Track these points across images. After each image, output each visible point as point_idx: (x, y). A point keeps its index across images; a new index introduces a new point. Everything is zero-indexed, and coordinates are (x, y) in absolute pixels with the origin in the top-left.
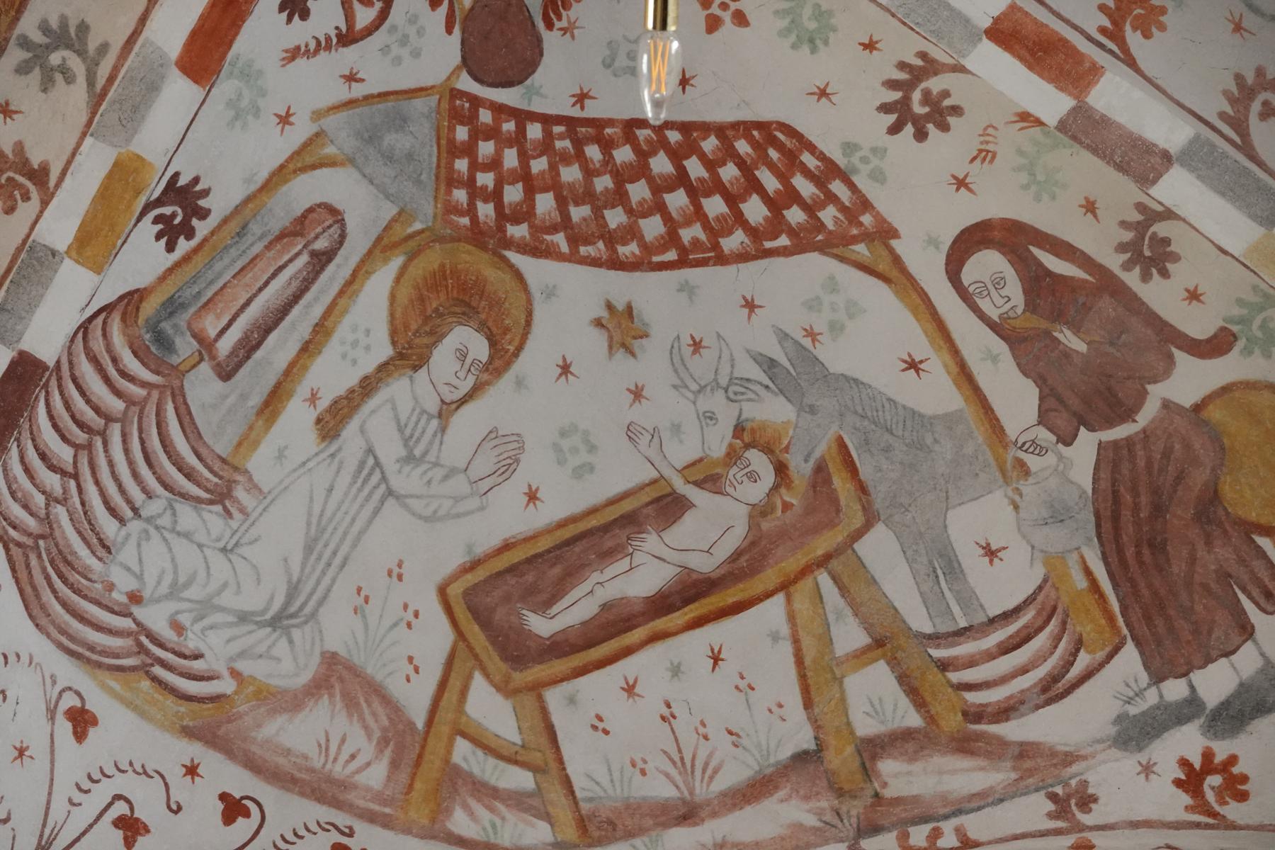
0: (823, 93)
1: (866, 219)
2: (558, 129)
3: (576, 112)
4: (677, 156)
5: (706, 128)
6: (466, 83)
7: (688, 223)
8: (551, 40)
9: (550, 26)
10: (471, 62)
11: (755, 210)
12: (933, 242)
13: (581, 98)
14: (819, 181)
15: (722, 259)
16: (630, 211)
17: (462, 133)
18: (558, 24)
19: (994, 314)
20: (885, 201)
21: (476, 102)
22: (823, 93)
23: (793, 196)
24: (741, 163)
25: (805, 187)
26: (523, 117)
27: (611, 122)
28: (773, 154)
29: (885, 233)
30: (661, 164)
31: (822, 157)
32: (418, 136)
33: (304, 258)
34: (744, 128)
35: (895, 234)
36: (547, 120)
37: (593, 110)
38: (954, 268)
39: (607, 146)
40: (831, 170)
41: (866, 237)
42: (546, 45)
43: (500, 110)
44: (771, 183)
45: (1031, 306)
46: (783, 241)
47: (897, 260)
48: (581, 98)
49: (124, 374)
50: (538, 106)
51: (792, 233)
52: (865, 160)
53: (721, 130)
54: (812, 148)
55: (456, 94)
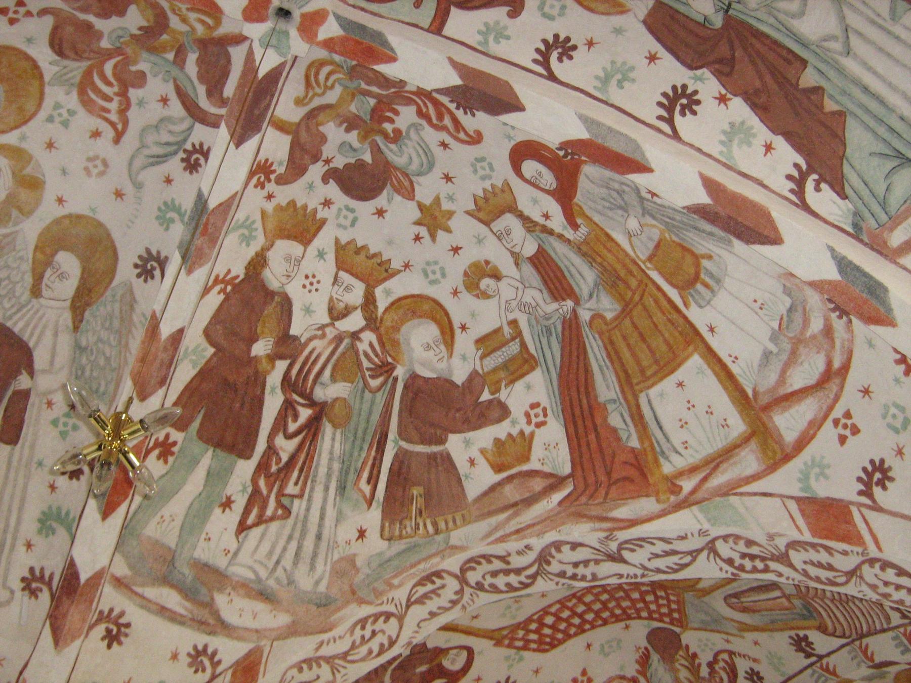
0: (537, 672)
1: (506, 642)
2: (635, 615)
3: (628, 622)
4: (584, 621)
5: (576, 634)
6: (677, 630)
7: (575, 605)
8: (644, 643)
9: (646, 649)
10: (677, 637)
11: (549, 620)
12: (480, 653)
13: (627, 627)
14: (528, 642)
15: (559, 602)
16: (599, 600)
17: (676, 615)
18: (643, 650)
19: (451, 652)
20: (504, 651)
21: (671, 623)
22: (537, 672)
23: (536, 631)
24: (559, 631)
25: (533, 636)
26: (650, 618)
27: (613, 623)
28: (548, 640)
29: (498, 643)
30: (590, 616)
31: (529, 649)
32: (694, 616)
33: (742, 600)
34: (561, 642)
35: (495, 645)
36: (640, 618)
37: (622, 624)
38: (470, 651)
39: (613, 615)
40: (525, 648)
41: (505, 637)
42: (646, 641)
43: (661, 621)
44: (547, 631)
45: (440, 665)
46: (535, 617)
47: (491, 638)
48: (627, 627)
49: (826, 610)
50: (646, 622)
51: (533, 621)
52: (513, 660)
53: (568, 636)
54: (534, 650)
55: (682, 627)
